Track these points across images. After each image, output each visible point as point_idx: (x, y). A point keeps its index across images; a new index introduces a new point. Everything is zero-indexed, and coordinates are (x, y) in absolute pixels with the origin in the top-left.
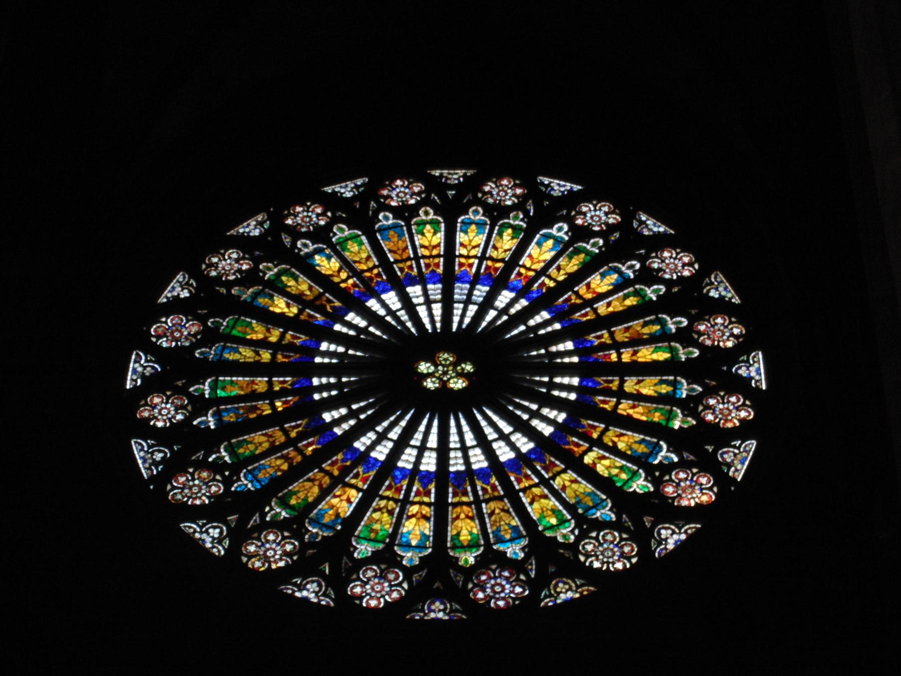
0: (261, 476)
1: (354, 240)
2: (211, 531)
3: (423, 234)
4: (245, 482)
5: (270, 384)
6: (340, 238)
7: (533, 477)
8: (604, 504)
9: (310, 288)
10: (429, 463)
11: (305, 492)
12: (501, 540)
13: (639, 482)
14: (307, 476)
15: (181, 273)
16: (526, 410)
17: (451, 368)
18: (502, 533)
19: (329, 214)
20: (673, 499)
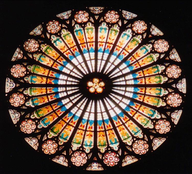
1: (68, 35)
2: (33, 140)
3: (88, 33)
5: (46, 89)
6: (64, 35)
8: (140, 131)
9: (56, 54)
10: (92, 118)
11: (58, 127)
12: (112, 144)
14: (58, 122)
15: (18, 48)
16: (118, 99)
17: (98, 84)
19: (60, 25)
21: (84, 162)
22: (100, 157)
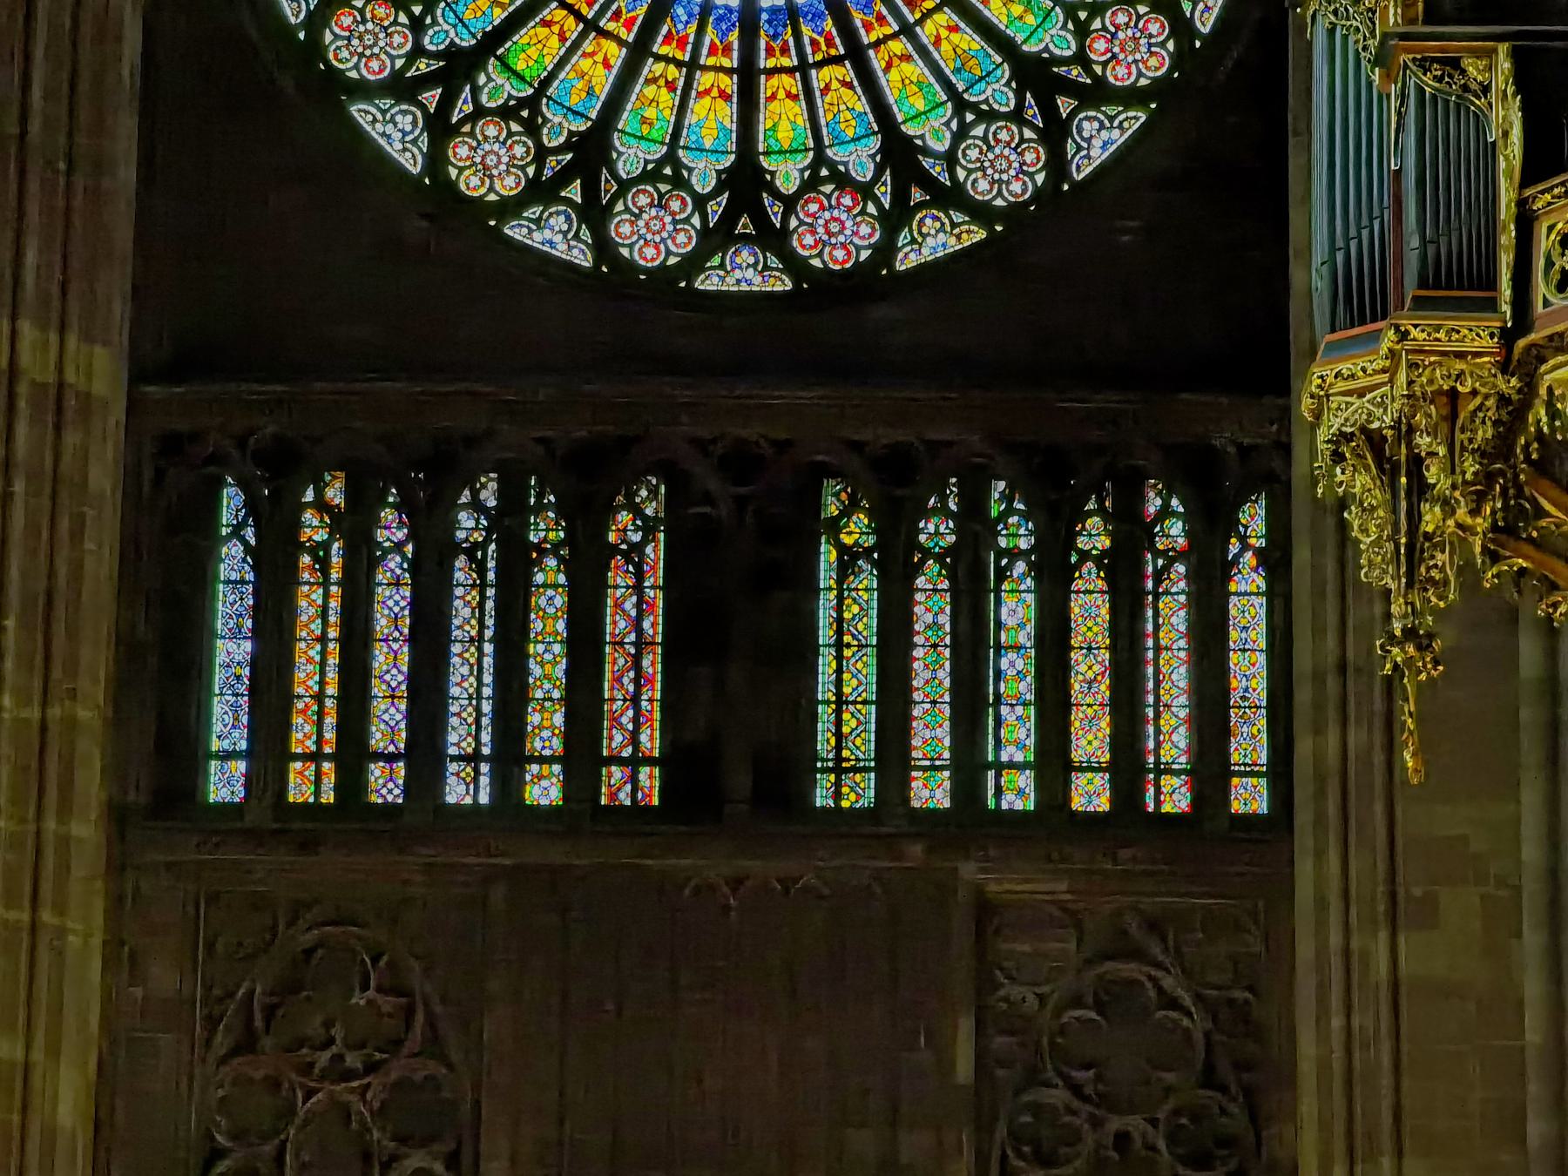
0: (468, 15)
2: (399, 118)
4: (446, 27)
7: (890, 19)
8: (999, 72)
11: (540, 46)
13: (1053, 32)
18: (843, 126)
20: (1105, 64)
21: (685, 242)
22: (775, 214)
